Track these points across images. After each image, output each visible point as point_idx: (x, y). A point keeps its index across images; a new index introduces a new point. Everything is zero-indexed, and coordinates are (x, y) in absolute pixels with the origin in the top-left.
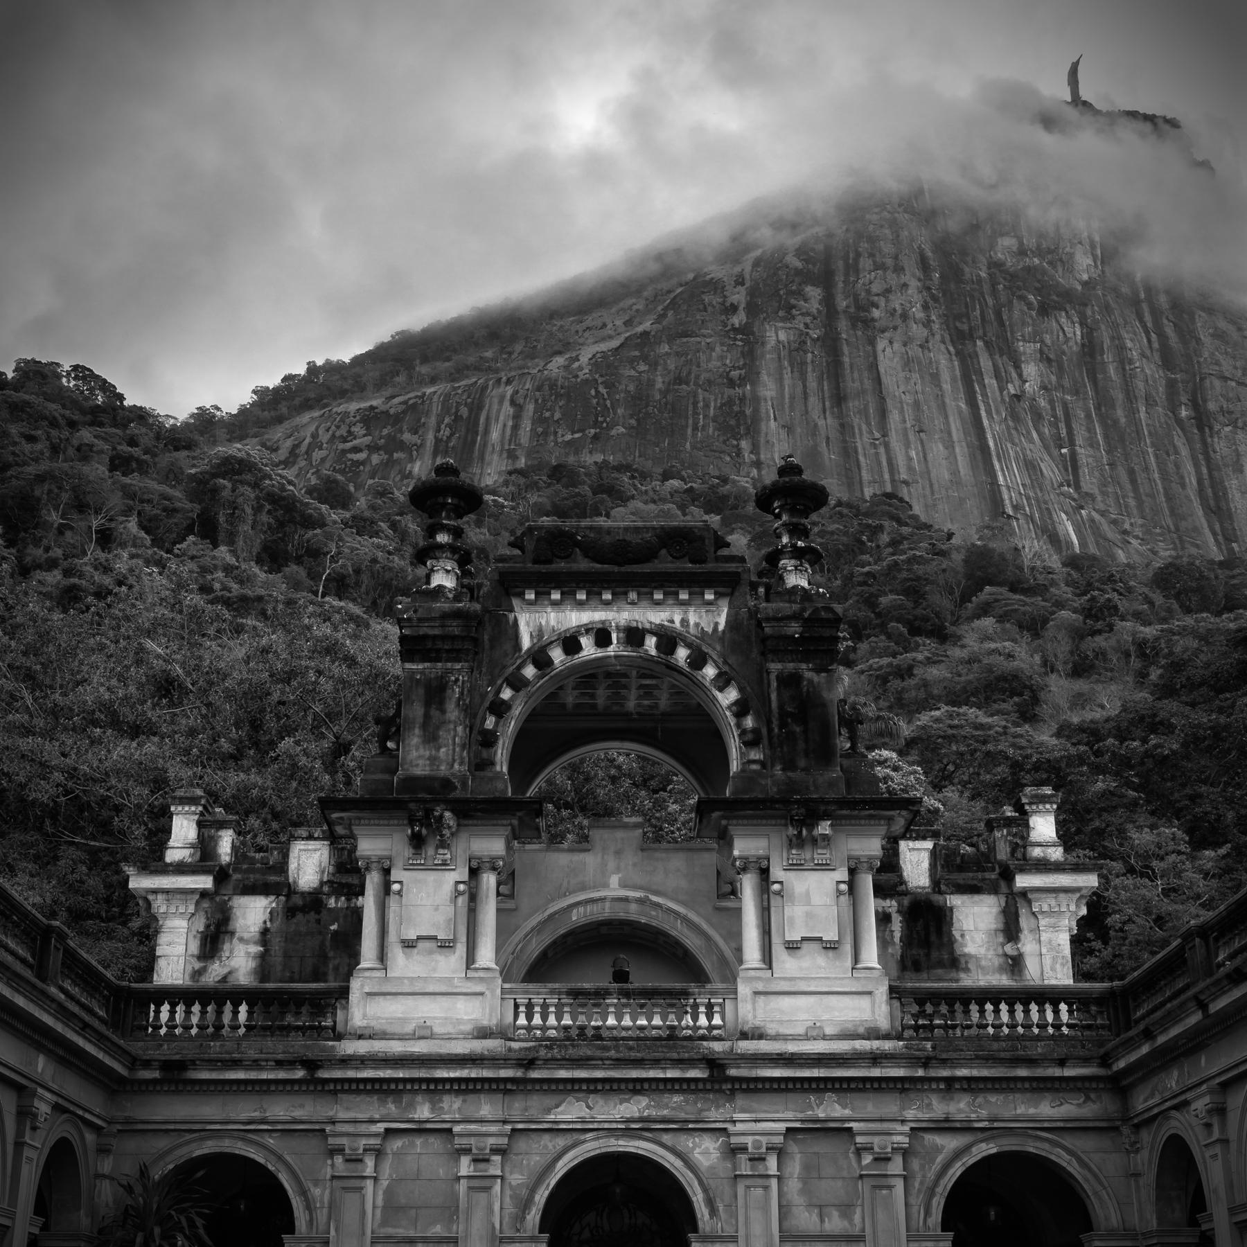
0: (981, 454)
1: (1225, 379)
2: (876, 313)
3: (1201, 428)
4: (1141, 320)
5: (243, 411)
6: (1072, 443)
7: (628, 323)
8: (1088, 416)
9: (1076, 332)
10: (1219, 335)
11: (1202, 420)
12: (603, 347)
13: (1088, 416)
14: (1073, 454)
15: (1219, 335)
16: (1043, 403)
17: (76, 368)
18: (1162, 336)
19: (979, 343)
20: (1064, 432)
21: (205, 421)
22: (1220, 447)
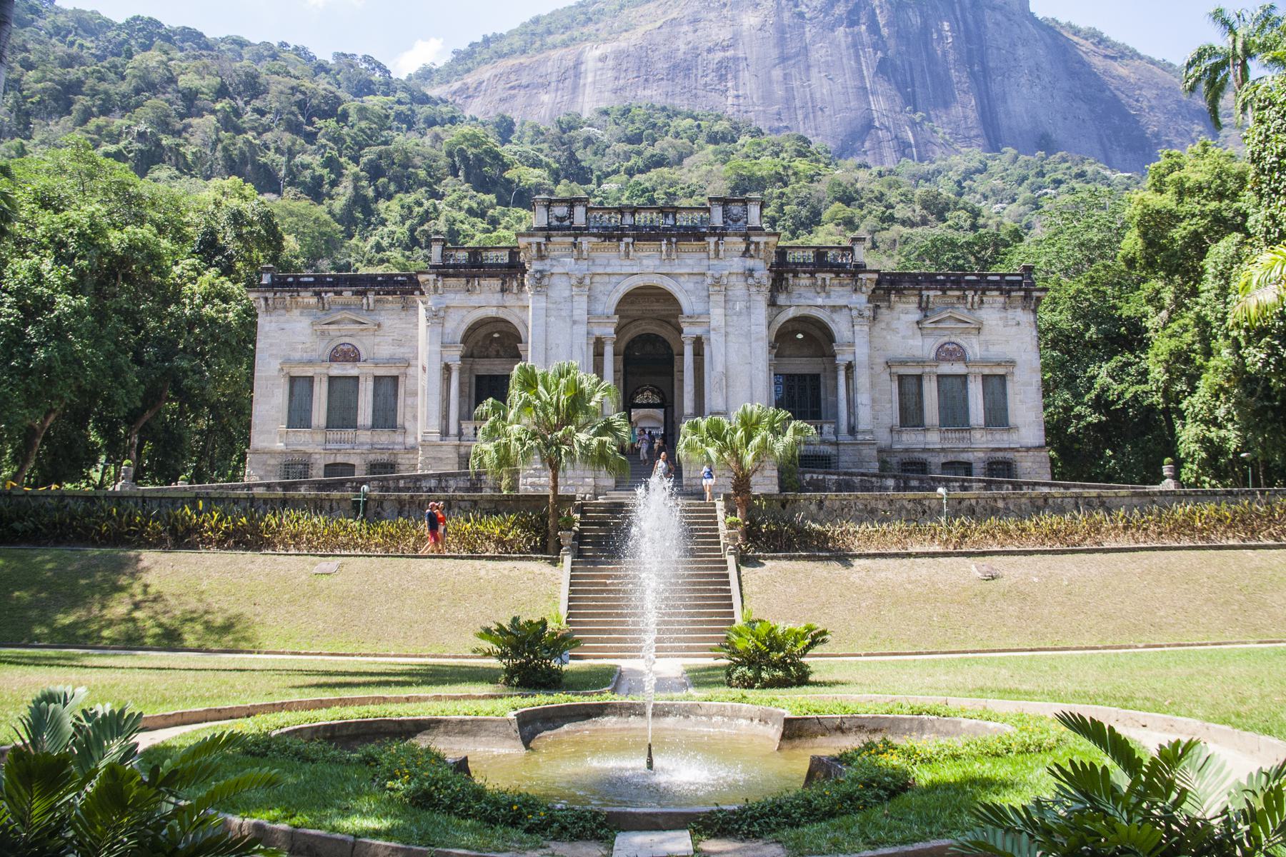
0: (863, 92)
1: (998, 49)
2: (803, 9)
3: (985, 77)
4: (954, 13)
5: (449, 65)
6: (913, 85)
7: (664, 13)
8: (923, 70)
9: (916, 20)
10: (997, 24)
11: (985, 70)
12: (650, 27)
13: (923, 70)
14: (914, 91)
15: (997, 24)
16: (898, 62)
17: (364, 57)
18: (965, 23)
19: (863, 27)
20: (909, 79)
21: (427, 74)
22: (995, 88)
